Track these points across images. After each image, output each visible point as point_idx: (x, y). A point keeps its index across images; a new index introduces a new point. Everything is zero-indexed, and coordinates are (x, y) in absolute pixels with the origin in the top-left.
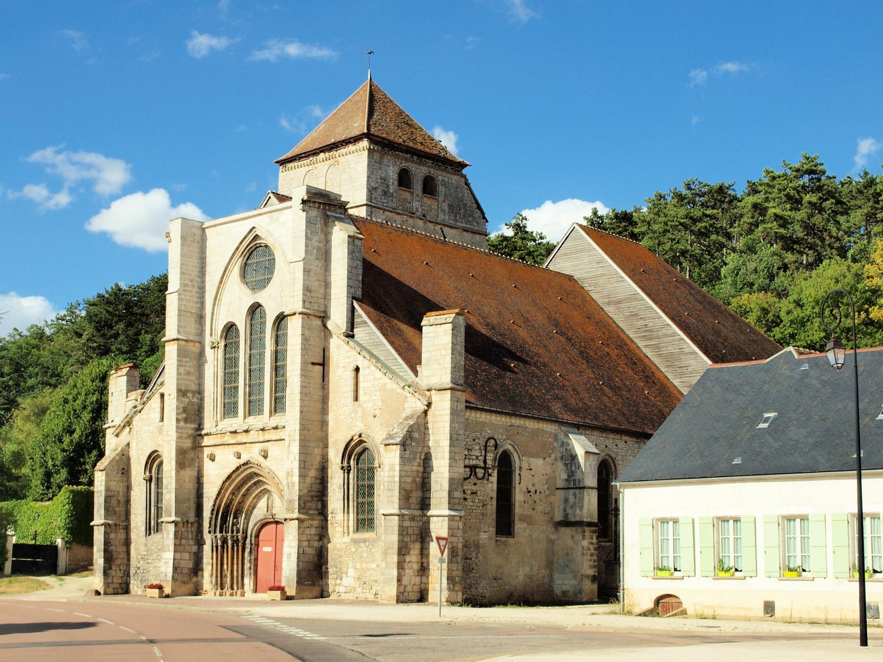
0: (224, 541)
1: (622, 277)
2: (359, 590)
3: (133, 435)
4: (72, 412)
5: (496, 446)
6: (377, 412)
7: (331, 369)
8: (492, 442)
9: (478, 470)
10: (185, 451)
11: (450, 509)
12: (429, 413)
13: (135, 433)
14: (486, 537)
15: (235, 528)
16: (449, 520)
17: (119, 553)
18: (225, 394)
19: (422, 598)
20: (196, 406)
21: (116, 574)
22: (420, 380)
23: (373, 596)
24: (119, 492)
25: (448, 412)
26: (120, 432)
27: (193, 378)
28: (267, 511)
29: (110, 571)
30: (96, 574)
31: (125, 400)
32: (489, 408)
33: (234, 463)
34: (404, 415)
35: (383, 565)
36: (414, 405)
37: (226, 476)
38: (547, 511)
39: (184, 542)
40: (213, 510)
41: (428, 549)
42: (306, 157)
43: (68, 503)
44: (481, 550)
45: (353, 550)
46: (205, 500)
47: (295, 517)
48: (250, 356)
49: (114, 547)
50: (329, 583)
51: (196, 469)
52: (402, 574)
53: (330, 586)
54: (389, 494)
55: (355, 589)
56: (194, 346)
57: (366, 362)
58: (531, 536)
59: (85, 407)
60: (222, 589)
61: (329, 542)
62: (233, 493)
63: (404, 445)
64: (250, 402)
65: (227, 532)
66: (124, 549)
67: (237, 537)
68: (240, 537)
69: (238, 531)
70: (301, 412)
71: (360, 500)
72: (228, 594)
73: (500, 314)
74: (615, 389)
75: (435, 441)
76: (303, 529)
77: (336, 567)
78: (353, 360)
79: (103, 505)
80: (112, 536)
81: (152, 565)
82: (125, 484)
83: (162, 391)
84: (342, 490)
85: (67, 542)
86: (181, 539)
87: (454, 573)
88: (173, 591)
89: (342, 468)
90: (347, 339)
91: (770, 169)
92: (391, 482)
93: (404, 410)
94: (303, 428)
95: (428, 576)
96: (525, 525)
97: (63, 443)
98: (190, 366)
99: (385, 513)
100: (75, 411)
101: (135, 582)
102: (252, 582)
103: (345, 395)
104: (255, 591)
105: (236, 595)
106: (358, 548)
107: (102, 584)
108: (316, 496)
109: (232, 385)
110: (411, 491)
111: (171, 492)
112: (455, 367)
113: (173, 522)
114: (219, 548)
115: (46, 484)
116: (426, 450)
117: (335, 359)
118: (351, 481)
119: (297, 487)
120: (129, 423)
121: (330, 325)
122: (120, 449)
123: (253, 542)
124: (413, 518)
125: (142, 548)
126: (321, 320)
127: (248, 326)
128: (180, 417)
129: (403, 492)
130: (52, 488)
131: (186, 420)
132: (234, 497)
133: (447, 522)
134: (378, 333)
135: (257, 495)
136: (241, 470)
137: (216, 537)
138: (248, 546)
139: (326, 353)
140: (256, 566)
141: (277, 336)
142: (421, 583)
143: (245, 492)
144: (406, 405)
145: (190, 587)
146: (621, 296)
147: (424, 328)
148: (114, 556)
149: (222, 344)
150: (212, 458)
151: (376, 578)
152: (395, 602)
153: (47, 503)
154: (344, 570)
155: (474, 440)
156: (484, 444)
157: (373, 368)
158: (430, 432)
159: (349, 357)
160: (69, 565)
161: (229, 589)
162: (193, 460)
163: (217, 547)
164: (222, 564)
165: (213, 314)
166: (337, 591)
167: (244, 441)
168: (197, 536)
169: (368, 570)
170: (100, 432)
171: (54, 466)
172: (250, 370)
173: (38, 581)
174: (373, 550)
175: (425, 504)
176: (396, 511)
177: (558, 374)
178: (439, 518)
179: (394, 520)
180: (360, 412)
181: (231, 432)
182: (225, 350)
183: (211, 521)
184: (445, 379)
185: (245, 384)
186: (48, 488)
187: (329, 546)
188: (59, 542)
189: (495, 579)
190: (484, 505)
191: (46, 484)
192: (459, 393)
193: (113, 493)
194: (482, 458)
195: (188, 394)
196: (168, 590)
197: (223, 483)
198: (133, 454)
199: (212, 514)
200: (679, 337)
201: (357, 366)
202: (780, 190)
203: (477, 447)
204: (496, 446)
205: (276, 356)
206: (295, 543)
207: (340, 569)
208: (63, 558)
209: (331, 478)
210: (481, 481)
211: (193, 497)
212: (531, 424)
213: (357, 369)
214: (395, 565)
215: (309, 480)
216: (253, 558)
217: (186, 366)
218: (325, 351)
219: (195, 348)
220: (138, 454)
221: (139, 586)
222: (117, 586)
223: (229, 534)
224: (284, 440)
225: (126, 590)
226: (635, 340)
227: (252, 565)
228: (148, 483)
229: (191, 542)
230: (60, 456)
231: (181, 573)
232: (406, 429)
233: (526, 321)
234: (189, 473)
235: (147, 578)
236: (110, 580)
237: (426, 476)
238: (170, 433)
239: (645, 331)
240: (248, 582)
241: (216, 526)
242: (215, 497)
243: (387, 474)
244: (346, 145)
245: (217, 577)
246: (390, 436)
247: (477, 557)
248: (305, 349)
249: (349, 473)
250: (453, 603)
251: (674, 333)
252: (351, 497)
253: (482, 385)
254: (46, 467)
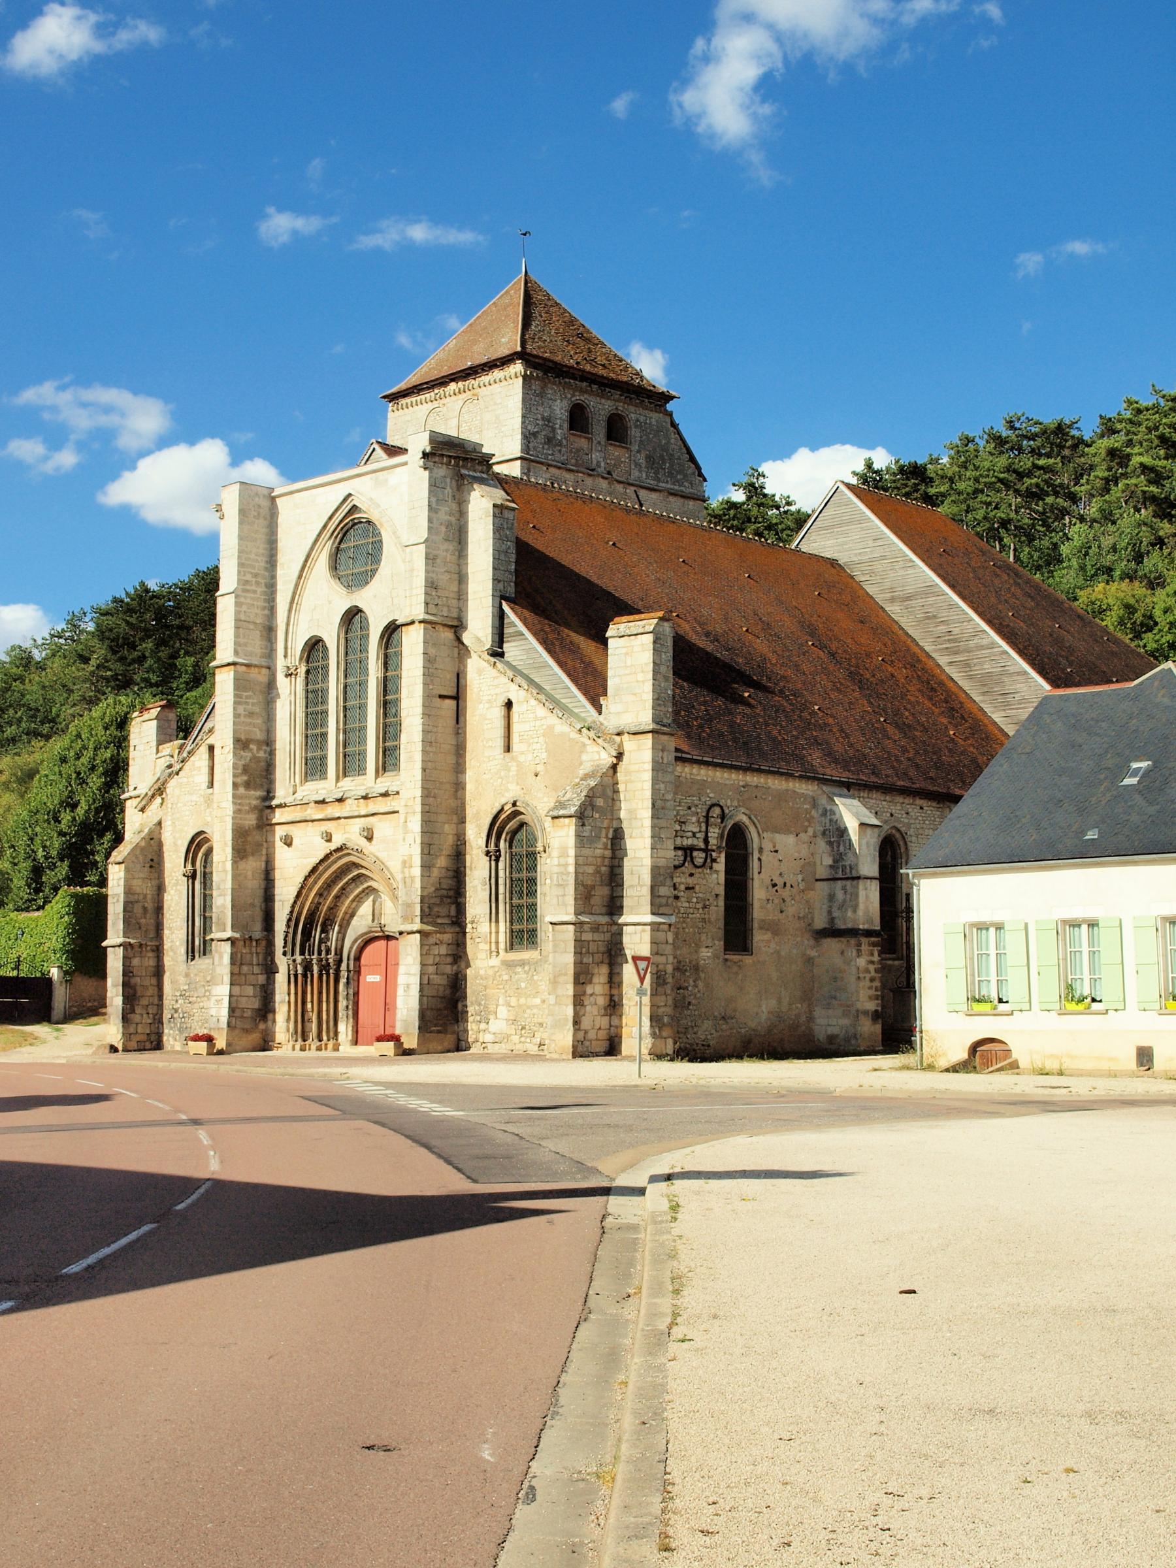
0: (307, 967)
1: (911, 561)
2: (515, 1038)
3: (167, 808)
4: (74, 776)
5: (723, 817)
6: (540, 768)
7: (469, 704)
8: (716, 811)
9: (695, 854)
10: (246, 831)
11: (653, 914)
12: (619, 769)
13: (170, 805)
14: (709, 954)
15: (323, 948)
16: (652, 930)
17: (145, 988)
18: (306, 745)
19: (612, 1048)
20: (263, 764)
21: (142, 1018)
22: (605, 719)
23: (536, 1048)
24: (145, 896)
25: (649, 766)
27: (259, 721)
28: (373, 920)
29: (132, 1015)
30: (112, 1022)
31: (155, 756)
32: (711, 760)
33: (322, 849)
34: (581, 772)
35: (552, 999)
36: (597, 757)
37: (309, 868)
38: (801, 915)
39: (245, 969)
40: (289, 920)
41: (620, 974)
43: (68, 914)
44: (702, 975)
45: (506, 977)
46: (278, 905)
47: (415, 929)
48: (345, 687)
49: (138, 979)
50: (469, 1028)
51: (264, 858)
52: (581, 1013)
53: (470, 1033)
54: (560, 891)
55: (508, 1036)
56: (259, 673)
57: (522, 693)
58: (778, 952)
59: (93, 768)
60: (304, 1041)
61: (468, 966)
62: (320, 894)
63: (581, 817)
64: (345, 756)
65: (311, 953)
66: (154, 981)
67: (327, 960)
68: (331, 961)
69: (328, 951)
70: (424, 770)
71: (515, 901)
72: (313, 1047)
73: (726, 618)
74: (904, 728)
75: (630, 811)
76: (427, 947)
77: (480, 1005)
78: (502, 690)
79: (121, 916)
80: (136, 962)
81: (196, 1005)
82: (155, 882)
83: (210, 741)
84: (488, 887)
85: (66, 973)
86: (241, 964)
87: (662, 1010)
88: (229, 1044)
89: (487, 853)
90: (493, 660)
91: (1135, 398)
92: (562, 873)
93: (581, 764)
94: (427, 794)
95: (621, 1016)
96: (768, 936)
97: (60, 822)
98: (253, 704)
99: (554, 921)
100: (79, 773)
102: (350, 1029)
103: (490, 743)
104: (356, 1042)
105: (326, 1049)
106: (513, 975)
107: (120, 1036)
108: (447, 897)
109: (318, 731)
110: (593, 887)
111: (225, 895)
112: (658, 699)
113: (228, 939)
114: (300, 977)
115: (34, 886)
116: (615, 824)
117: (475, 690)
118: (501, 873)
119: (418, 884)
120: (160, 791)
121: (467, 638)
122: (146, 831)
123: (351, 968)
124: (596, 928)
125: (182, 980)
126: (453, 631)
127: (342, 641)
128: (239, 780)
129: (581, 888)
130: (43, 891)
131: (247, 785)
132: (321, 900)
133: (649, 933)
134: (540, 649)
135: (357, 896)
136: (332, 858)
137: (294, 961)
138: (344, 974)
139: (461, 680)
140: (356, 1004)
141: (386, 656)
142: (611, 1026)
143: (338, 892)
144: (584, 757)
145: (255, 1037)
146: (910, 589)
147: (610, 641)
148: (139, 994)
149: (303, 669)
150: (289, 841)
151: (540, 1021)
152: (570, 1057)
153: (36, 914)
154: (492, 1008)
155: (689, 808)
156: (704, 814)
157: (533, 702)
158: (622, 798)
159: (497, 686)
160: (70, 1007)
161: (316, 1040)
162: (259, 845)
163: (296, 976)
164: (304, 1003)
165: (288, 625)
166: (481, 1040)
167: (337, 815)
168: (265, 959)
169: (528, 1007)
170: (117, 806)
171: (46, 858)
172: (345, 707)
173: (22, 1032)
174: (535, 978)
175: (614, 906)
176: (571, 917)
177: (816, 707)
178: (637, 927)
179: (567, 931)
180: (514, 769)
181: (316, 802)
182: (307, 678)
183: (286, 936)
184: (645, 718)
185: (338, 729)
186: (37, 891)
187: (469, 971)
188: (54, 973)
189: (723, 1018)
190: (705, 907)
191: (34, 886)
192: (665, 737)
193: (136, 897)
194: (701, 835)
195: (251, 746)
196: (221, 1043)
197: (306, 879)
198: (167, 837)
199: (288, 926)
200: (1001, 649)
201: (509, 700)
202: (1149, 430)
203: (694, 819)
204: (723, 817)
205: (385, 686)
206: (416, 969)
207: (486, 1007)
208: (60, 997)
209: (471, 870)
210: (700, 870)
211: (258, 902)
212: (776, 784)
213: (509, 704)
214: (570, 1001)
215: (436, 873)
216: (351, 992)
217: (247, 703)
218: (459, 678)
219: (261, 677)
220: (174, 838)
221: (178, 1038)
222: (144, 1038)
223: (315, 956)
224: (398, 812)
225: (158, 1045)
226: (934, 655)
227: (351, 1002)
228: (190, 881)
229: (257, 970)
230: (57, 843)
231: (242, 1017)
232: (584, 793)
233: (767, 627)
234: (253, 865)
235: (189, 1025)
236: (132, 1030)
237: (617, 864)
238: (223, 805)
239: (949, 640)
240: (346, 1030)
241: (294, 944)
242: (292, 901)
243: (556, 862)
245: (296, 1022)
246: (561, 805)
247: (696, 986)
248: (429, 674)
249: (497, 861)
250: (659, 1056)
251: (993, 644)
252: (501, 897)
253: (701, 726)
254: (34, 860)
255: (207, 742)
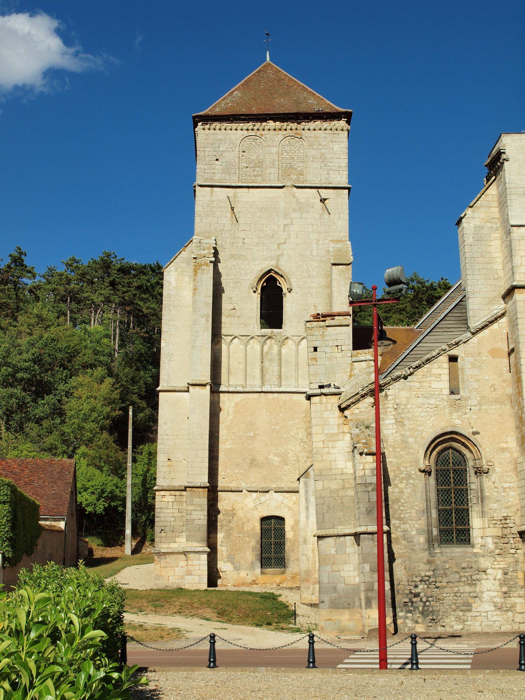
26: (353, 403)
42: (244, 120)
83: (453, 352)
101: (409, 615)
221: (420, 620)
244: (311, 120)
255: (448, 353)
